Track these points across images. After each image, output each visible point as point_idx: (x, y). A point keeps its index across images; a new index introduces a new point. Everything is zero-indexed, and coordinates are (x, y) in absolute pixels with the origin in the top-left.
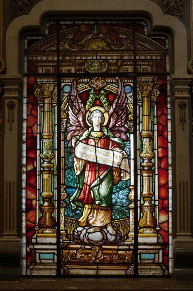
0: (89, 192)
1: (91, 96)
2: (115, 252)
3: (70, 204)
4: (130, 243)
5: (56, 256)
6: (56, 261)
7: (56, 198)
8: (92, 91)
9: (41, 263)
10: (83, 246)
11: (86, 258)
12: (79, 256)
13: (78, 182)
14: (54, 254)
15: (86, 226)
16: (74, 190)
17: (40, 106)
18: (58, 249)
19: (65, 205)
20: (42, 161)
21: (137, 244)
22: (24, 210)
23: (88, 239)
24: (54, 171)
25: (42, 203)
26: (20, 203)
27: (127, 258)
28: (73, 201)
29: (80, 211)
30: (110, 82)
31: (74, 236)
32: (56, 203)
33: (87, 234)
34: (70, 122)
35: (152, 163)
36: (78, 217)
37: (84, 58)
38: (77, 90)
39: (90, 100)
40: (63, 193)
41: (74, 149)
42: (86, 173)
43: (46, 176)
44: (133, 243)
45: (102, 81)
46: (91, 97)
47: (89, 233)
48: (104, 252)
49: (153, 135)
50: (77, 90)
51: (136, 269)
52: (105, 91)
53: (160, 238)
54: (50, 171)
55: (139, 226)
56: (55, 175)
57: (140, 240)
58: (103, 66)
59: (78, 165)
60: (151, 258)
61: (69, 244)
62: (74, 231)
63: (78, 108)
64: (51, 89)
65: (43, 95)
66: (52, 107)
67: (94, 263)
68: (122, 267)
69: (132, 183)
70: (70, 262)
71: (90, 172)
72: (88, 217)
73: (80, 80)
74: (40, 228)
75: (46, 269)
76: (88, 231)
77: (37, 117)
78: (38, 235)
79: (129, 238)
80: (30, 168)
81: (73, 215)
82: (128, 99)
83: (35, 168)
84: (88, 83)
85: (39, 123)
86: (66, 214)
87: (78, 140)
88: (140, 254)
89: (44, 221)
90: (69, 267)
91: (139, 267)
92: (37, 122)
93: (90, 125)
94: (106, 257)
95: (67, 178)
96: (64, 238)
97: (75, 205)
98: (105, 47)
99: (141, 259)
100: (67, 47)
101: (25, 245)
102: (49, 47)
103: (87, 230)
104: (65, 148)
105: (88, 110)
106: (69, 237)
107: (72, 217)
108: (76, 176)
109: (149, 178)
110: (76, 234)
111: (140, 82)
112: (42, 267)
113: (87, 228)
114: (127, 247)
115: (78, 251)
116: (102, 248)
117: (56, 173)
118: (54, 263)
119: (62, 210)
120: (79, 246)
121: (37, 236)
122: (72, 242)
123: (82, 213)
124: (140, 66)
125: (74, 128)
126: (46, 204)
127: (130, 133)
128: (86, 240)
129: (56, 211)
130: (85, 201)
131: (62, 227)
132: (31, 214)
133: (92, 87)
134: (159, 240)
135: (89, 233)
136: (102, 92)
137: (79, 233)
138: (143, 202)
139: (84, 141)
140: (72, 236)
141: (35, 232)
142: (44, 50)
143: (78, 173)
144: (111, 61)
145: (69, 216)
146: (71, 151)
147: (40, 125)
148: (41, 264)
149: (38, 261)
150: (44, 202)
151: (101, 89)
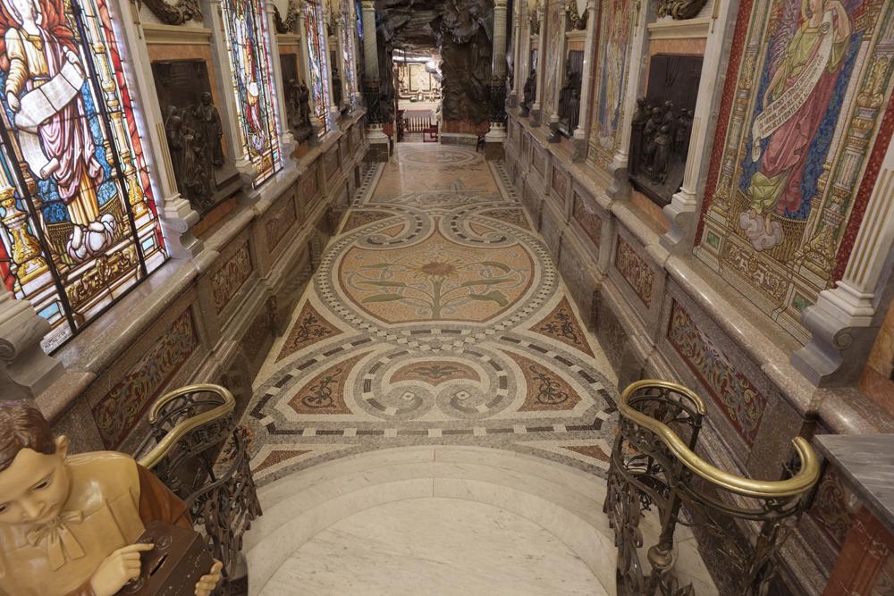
5: (60, 304)
6: (63, 313)
14: (56, 301)
18: (61, 290)
21: (134, 232)
48: (110, 261)
70: (80, 303)
106: (63, 261)
114: (127, 241)
118: (62, 317)
121: (21, 285)
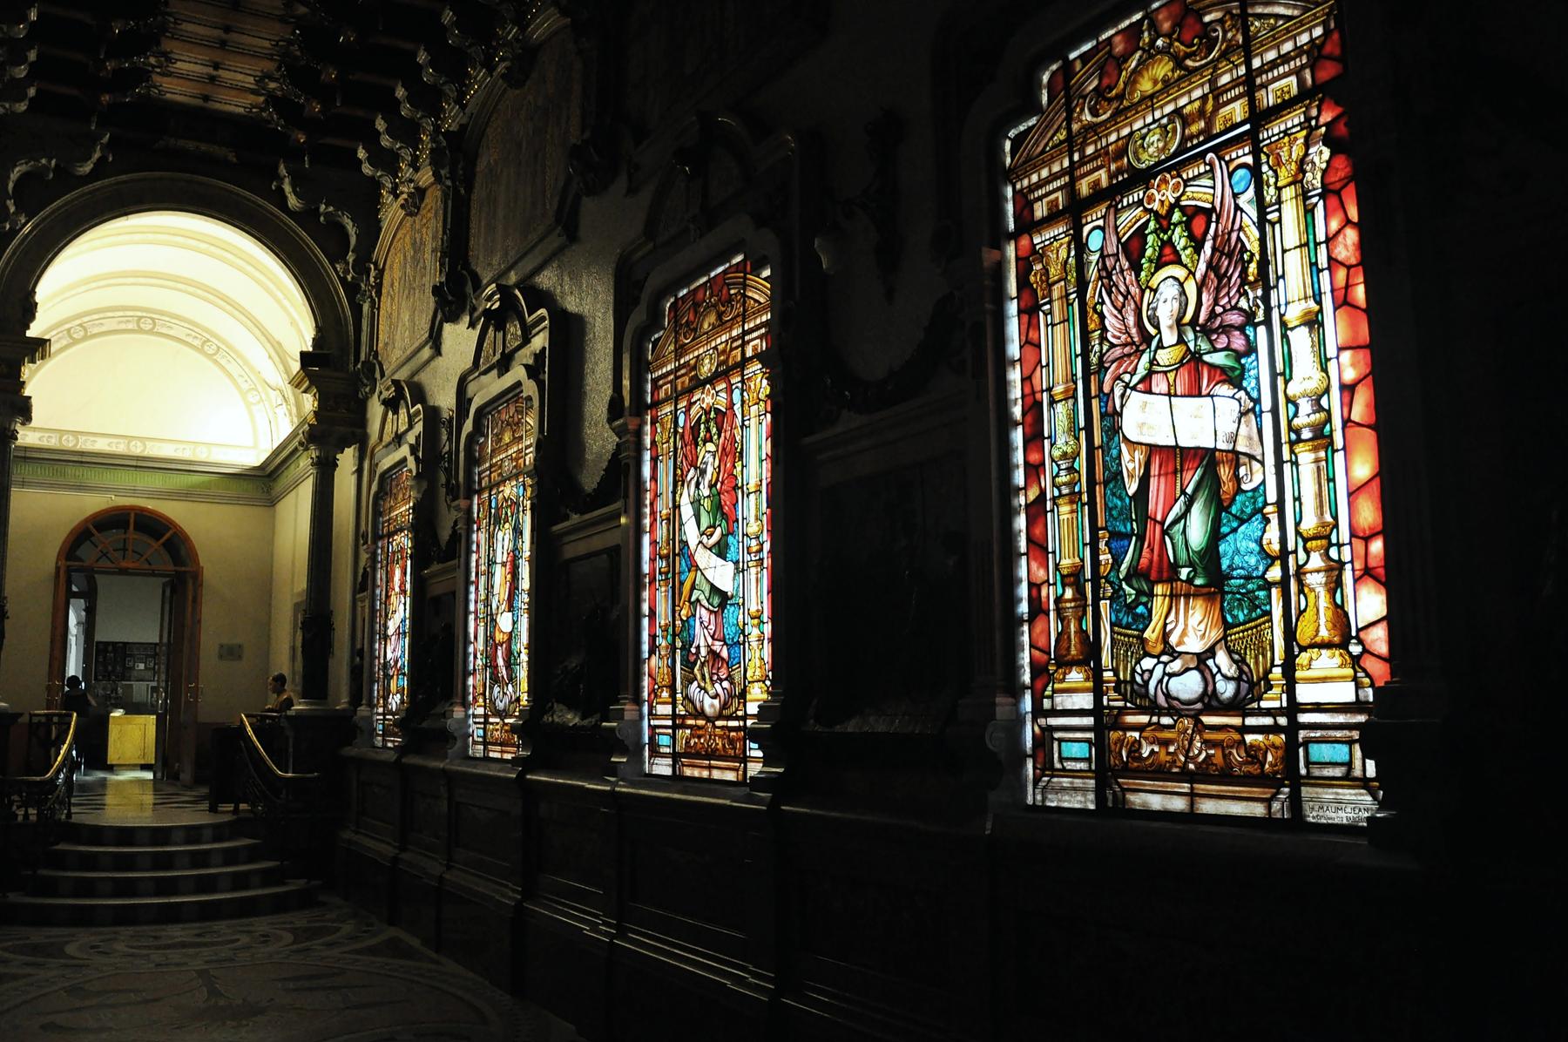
0: (1163, 542)
1: (1150, 239)
2: (1236, 736)
3: (1121, 587)
4: (1276, 704)
7: (1088, 575)
8: (1152, 225)
9: (1064, 769)
10: (1155, 719)
11: (1163, 757)
12: (1145, 752)
13: (1134, 517)
15: (1163, 653)
16: (1126, 543)
17: (1043, 312)
18: (1098, 728)
19: (1109, 593)
20: (1056, 469)
22: (1026, 617)
23: (1168, 696)
24: (1080, 493)
25: (1060, 591)
26: (1013, 601)
27: (1270, 758)
28: (1128, 579)
29: (1145, 605)
30: (1194, 178)
31: (1136, 687)
32: (1089, 586)
33: (1166, 678)
34: (1109, 336)
35: (1324, 410)
36: (1141, 626)
37: (1125, 132)
38: (1117, 233)
39: (1149, 252)
40: (1105, 557)
41: (1120, 415)
42: (1153, 483)
43: (1065, 509)
44: (1285, 704)
45: (1174, 181)
46: (1150, 244)
47: (1171, 675)
48: (1209, 735)
49: (1321, 311)
50: (1117, 233)
51: (1296, 802)
52: (1183, 209)
53: (1362, 683)
54: (1074, 497)
55: (1298, 644)
56: (1083, 505)
57: (1304, 694)
58: (1170, 135)
59: (1131, 463)
60: (1339, 761)
61: (1123, 711)
62: (1133, 671)
63: (1123, 289)
64: (1063, 253)
65: (1048, 278)
66: (1068, 305)
67: (1185, 776)
68: (1256, 791)
69: (1272, 496)
70: (1126, 771)
71: (1163, 479)
72: (1165, 625)
73: (1121, 201)
74: (1059, 665)
75: (1075, 789)
76: (1168, 670)
77: (1039, 346)
78: (1056, 686)
79: (1270, 687)
80: (1033, 493)
81: (1130, 620)
82: (1242, 211)
83: (1043, 493)
84: (1140, 203)
85: (1044, 363)
86: (1114, 619)
87: (1127, 386)
88: (1307, 742)
89: (1065, 645)
90: (1126, 784)
91: (1306, 792)
92: (1040, 361)
93: (1153, 331)
94: (1213, 755)
95: (1111, 509)
96: (1112, 694)
97: (1133, 589)
98: (1170, 74)
99: (1308, 763)
100: (1087, 117)
101: (1029, 717)
102: (1051, 138)
103: (1166, 664)
104: (1103, 416)
105: (1147, 287)
107: (1128, 627)
108: (1127, 500)
109: (1318, 468)
110: (1138, 679)
111: (1268, 141)
112: (1066, 782)
113: (1165, 658)
114: (1268, 721)
115: (1144, 734)
116: (1202, 722)
117: (1085, 498)
118: (1090, 770)
119: (1104, 605)
120: (1144, 719)
121: (1054, 691)
122: (1129, 705)
123: (1150, 611)
124: (1264, 86)
125: (1118, 352)
126: (1069, 594)
127: (1255, 326)
128: (1161, 700)
129: (1090, 610)
130: (1153, 576)
131: (1106, 658)
132: (1039, 626)
133: (1151, 211)
134: (1360, 692)
135: (1171, 675)
136: (1176, 216)
137: (1146, 676)
138: (1305, 557)
139: (1140, 386)
140: (1129, 688)
141: (1050, 678)
142: (1043, 152)
143: (1132, 488)
144: (1189, 108)
145: (1120, 626)
146: (1113, 419)
147: (1048, 365)
148: (1065, 772)
149: (1058, 765)
150: (1064, 586)
151: (1172, 207)
